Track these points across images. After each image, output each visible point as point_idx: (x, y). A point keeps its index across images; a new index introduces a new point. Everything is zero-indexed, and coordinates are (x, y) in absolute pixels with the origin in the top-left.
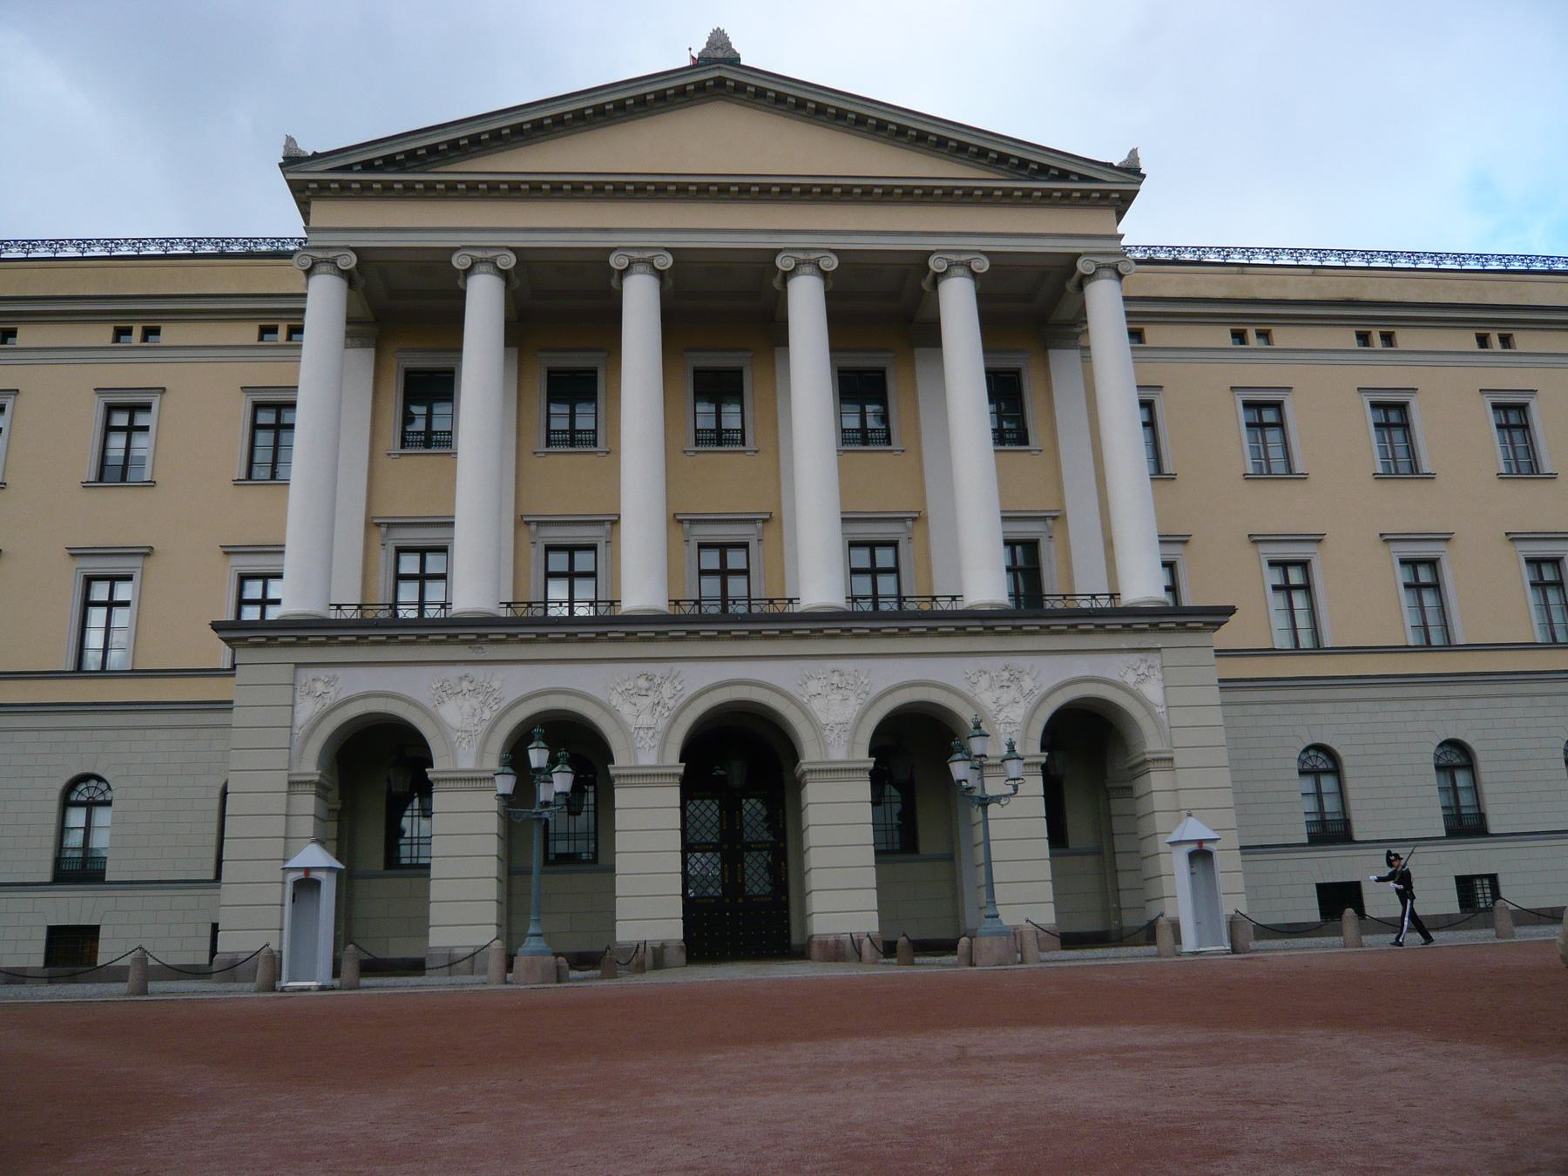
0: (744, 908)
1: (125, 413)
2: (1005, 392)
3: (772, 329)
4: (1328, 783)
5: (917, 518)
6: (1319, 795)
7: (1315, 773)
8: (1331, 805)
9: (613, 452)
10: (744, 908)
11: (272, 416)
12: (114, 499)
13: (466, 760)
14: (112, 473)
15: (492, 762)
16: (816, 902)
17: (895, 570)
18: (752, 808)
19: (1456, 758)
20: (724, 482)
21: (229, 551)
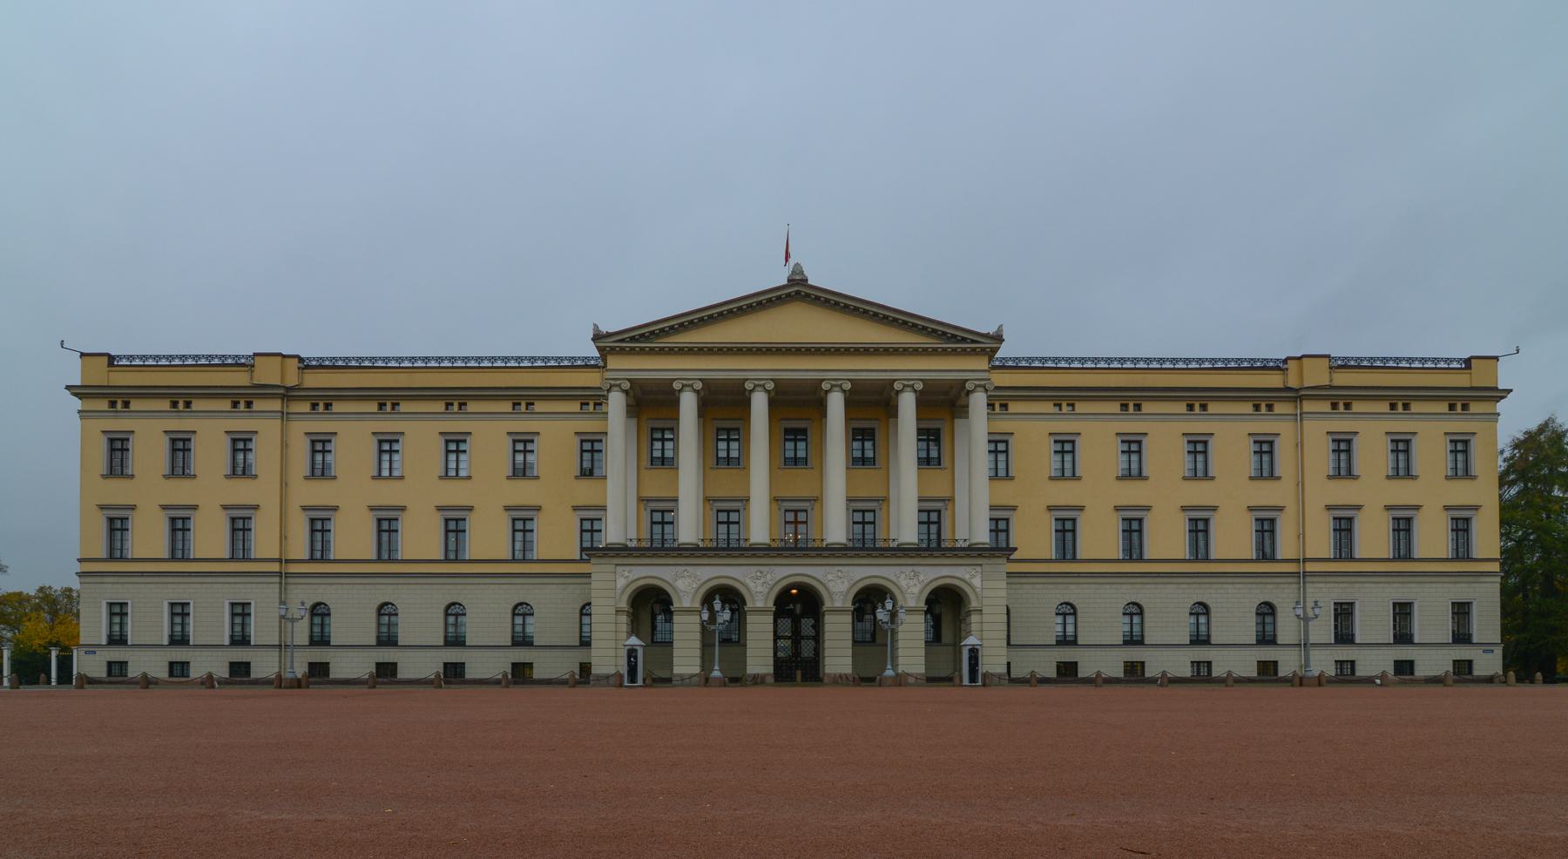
0: (800, 666)
1: (522, 443)
2: (929, 435)
3: (821, 406)
4: (1070, 619)
5: (885, 500)
6: (1065, 624)
7: (1065, 615)
8: (1070, 629)
9: (747, 468)
10: (800, 666)
11: (591, 446)
12: (521, 485)
13: (686, 604)
14: (521, 472)
15: (697, 605)
16: (827, 661)
17: (873, 523)
18: (807, 625)
19: (1135, 610)
20: (798, 484)
21: (576, 508)
